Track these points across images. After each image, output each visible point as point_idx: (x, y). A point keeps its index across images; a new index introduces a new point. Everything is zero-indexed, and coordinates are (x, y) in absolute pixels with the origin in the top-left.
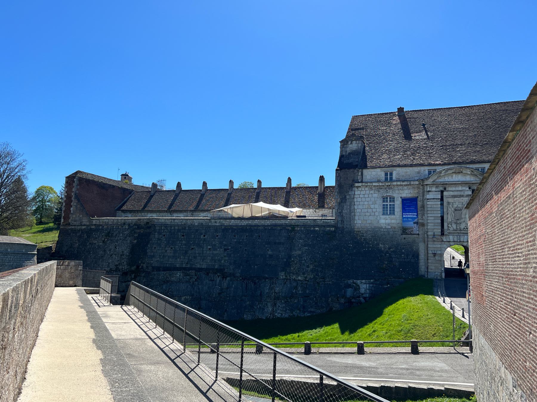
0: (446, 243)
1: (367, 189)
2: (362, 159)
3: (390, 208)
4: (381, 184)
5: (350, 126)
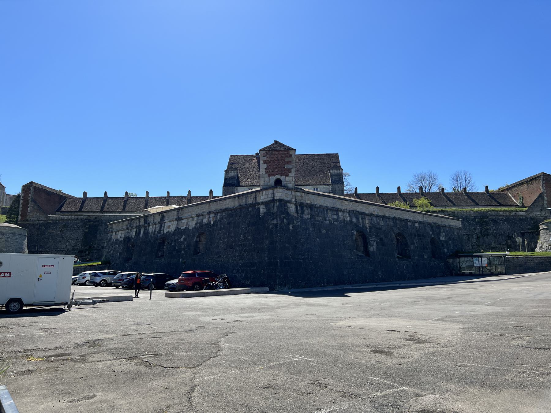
5: (229, 161)
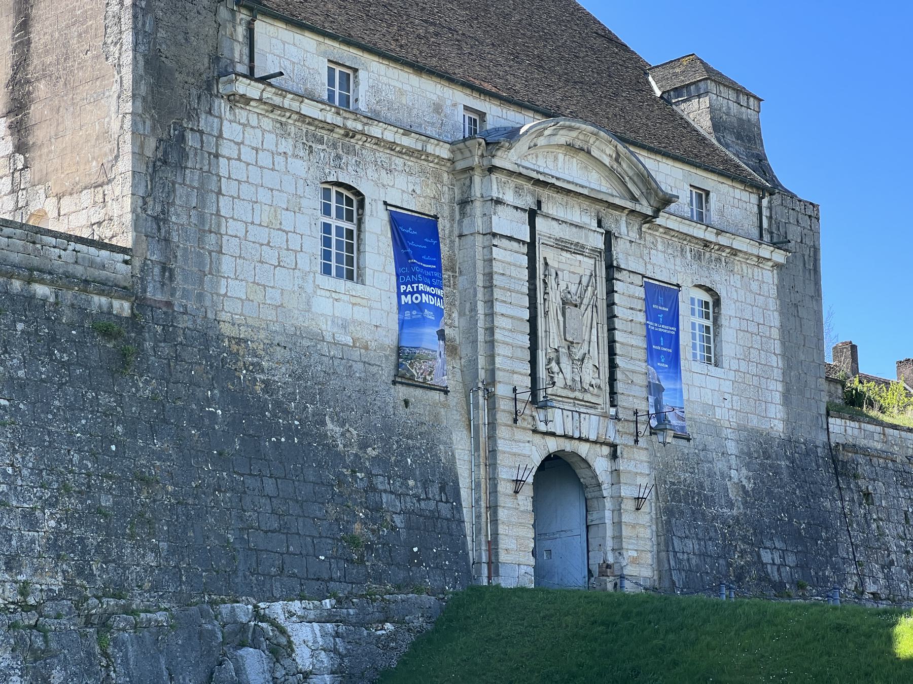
1: (267, 123)
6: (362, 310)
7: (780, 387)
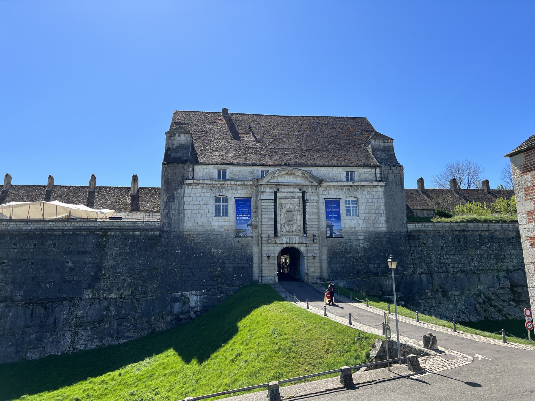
0: (279, 245)
2: (192, 155)
3: (223, 209)
4: (214, 182)
5: (173, 120)
6: (227, 223)
7: (384, 219)
